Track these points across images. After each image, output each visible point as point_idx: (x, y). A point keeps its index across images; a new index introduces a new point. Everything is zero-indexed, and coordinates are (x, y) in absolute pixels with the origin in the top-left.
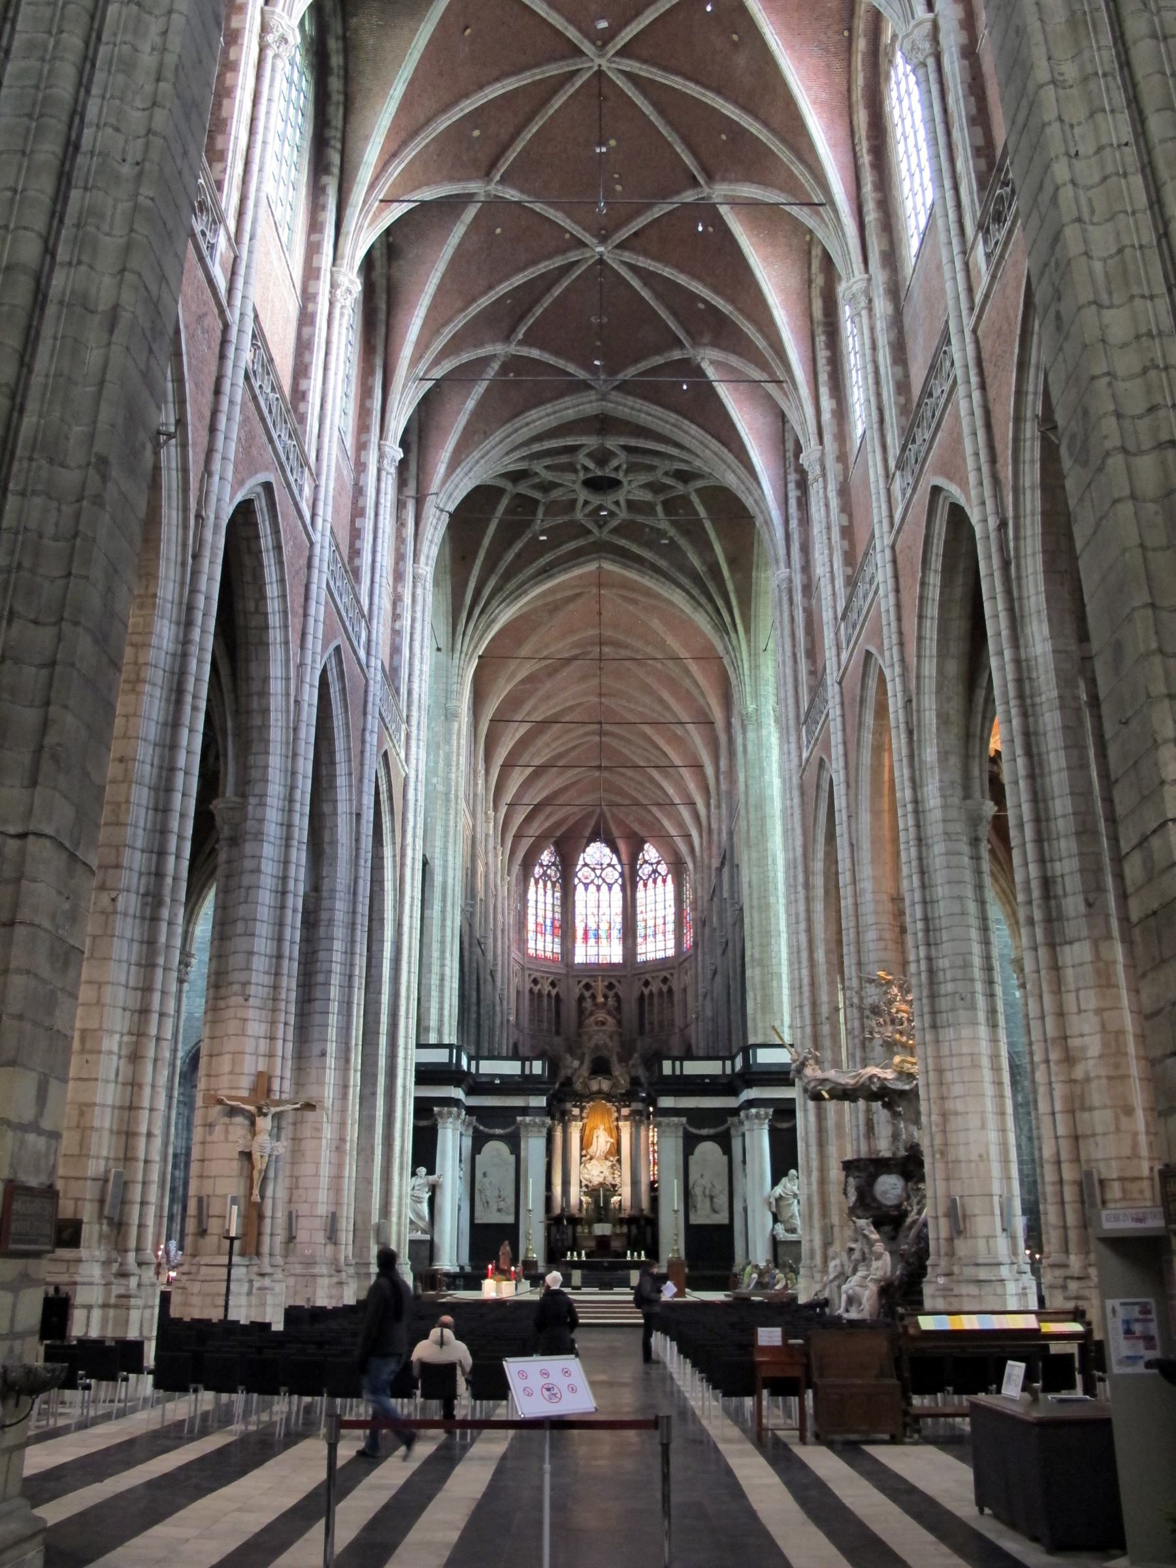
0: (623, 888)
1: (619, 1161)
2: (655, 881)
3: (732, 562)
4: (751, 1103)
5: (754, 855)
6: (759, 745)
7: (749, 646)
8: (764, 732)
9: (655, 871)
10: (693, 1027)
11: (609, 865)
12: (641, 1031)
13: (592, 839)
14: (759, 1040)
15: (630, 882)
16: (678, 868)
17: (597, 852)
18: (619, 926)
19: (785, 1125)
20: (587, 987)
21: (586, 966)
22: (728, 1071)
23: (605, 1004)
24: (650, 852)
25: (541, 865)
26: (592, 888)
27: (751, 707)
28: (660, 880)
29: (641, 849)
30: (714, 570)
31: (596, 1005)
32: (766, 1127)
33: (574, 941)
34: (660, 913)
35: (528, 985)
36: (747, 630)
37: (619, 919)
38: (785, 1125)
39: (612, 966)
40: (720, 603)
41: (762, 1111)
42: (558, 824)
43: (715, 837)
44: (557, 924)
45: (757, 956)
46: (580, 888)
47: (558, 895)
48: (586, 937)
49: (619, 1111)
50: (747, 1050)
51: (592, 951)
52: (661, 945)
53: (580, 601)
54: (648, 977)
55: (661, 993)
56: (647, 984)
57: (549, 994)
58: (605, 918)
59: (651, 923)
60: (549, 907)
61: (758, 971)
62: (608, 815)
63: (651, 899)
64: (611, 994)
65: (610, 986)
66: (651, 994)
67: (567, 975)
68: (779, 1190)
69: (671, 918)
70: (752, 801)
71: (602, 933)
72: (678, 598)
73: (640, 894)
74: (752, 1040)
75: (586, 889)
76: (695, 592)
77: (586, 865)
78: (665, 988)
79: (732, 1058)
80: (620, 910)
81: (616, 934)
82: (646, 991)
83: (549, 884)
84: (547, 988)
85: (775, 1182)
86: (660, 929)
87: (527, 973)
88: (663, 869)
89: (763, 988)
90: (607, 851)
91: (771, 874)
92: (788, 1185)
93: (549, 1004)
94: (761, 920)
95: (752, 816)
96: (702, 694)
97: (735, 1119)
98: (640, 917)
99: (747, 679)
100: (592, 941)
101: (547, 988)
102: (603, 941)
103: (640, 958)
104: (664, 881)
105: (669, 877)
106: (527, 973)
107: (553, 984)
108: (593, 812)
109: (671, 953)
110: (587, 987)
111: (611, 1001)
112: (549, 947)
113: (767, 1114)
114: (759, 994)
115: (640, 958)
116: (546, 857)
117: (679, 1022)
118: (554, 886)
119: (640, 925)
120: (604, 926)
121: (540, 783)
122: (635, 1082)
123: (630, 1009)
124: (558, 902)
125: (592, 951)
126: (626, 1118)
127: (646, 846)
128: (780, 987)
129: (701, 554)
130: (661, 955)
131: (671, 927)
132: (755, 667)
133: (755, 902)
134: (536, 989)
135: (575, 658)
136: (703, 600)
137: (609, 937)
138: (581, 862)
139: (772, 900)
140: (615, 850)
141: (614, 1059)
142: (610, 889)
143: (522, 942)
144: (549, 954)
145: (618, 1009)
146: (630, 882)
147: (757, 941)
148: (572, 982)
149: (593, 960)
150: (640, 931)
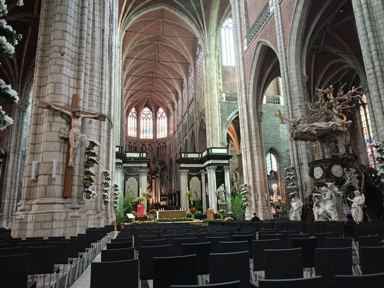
0: (153, 120)
1: (152, 189)
2: (162, 118)
3: (204, 7)
4: (209, 165)
5: (209, 95)
6: (210, 63)
7: (208, 35)
8: (212, 59)
9: (161, 115)
10: (173, 154)
11: (149, 114)
12: (158, 156)
13: (145, 107)
14: (211, 147)
15: (155, 118)
16: (168, 114)
17: (146, 110)
18: (152, 129)
19: (219, 171)
20: (144, 145)
21: (143, 139)
22: (200, 157)
23: (149, 149)
24: (161, 110)
25: (132, 113)
26: (145, 119)
27: (208, 52)
28: (163, 117)
29: (158, 110)
30: (199, 9)
31: (146, 149)
32: (215, 171)
33: (140, 133)
34: (163, 126)
35: (128, 143)
36: (208, 30)
37: (152, 128)
38: (219, 171)
39: (150, 140)
40: (200, 20)
41: (214, 166)
42: (136, 101)
43: (185, 101)
44: (136, 128)
45: (210, 123)
46: (142, 119)
47: (136, 121)
48: (143, 132)
49: (152, 177)
50: (208, 150)
51: (145, 135)
52: (163, 134)
53: (153, 23)
54: (160, 142)
55: (163, 146)
56: (159, 144)
57: (133, 146)
58: (148, 127)
59: (160, 129)
60: (134, 124)
61: (210, 128)
62: (150, 99)
63: (160, 123)
64: (150, 147)
65: (150, 145)
66: (160, 146)
67: (138, 141)
68: (219, 190)
69: (166, 127)
70: (208, 79)
71: (147, 131)
72: (186, 20)
73: (158, 121)
74: (208, 147)
75: (143, 120)
76: (192, 17)
77: (143, 113)
78: (164, 145)
79: (202, 153)
80: (152, 125)
81: (151, 131)
82: (159, 146)
83: (134, 117)
84: (133, 144)
85: (218, 188)
86: (163, 130)
87: (128, 140)
88: (164, 114)
89: (212, 132)
90: (149, 110)
91: (215, 100)
92: (221, 188)
93: (134, 149)
94: (211, 113)
95: (208, 83)
96: (188, 55)
97: (203, 170)
98: (157, 127)
99: (207, 44)
100: (145, 133)
101: (133, 144)
102: (148, 133)
103: (158, 138)
104: (164, 118)
105: (166, 117)
106: (128, 140)
107: (135, 144)
108: (146, 98)
109: (166, 136)
110: (144, 145)
111: (150, 148)
112: (134, 134)
113: (215, 168)
114: (211, 134)
115: (158, 138)
116: (133, 110)
117: (168, 153)
118: (135, 118)
119: (158, 129)
120: (148, 129)
121: (134, 86)
122: (157, 168)
123: (155, 150)
124: (136, 122)
125: (145, 135)
126: (154, 178)
127: (159, 109)
128: (217, 132)
129: (195, 5)
130: (163, 137)
131: (166, 130)
132: (209, 41)
133: (209, 108)
134: (130, 145)
135: (150, 44)
136: (194, 20)
137: (149, 132)
138: (142, 113)
139: (215, 107)
140: (151, 110)
141: (151, 162)
142: (150, 120)
143: (127, 132)
144: (134, 136)
145: (152, 150)
146: (155, 118)
147: (210, 119)
148: (140, 143)
149: (145, 138)
150: (158, 131)
